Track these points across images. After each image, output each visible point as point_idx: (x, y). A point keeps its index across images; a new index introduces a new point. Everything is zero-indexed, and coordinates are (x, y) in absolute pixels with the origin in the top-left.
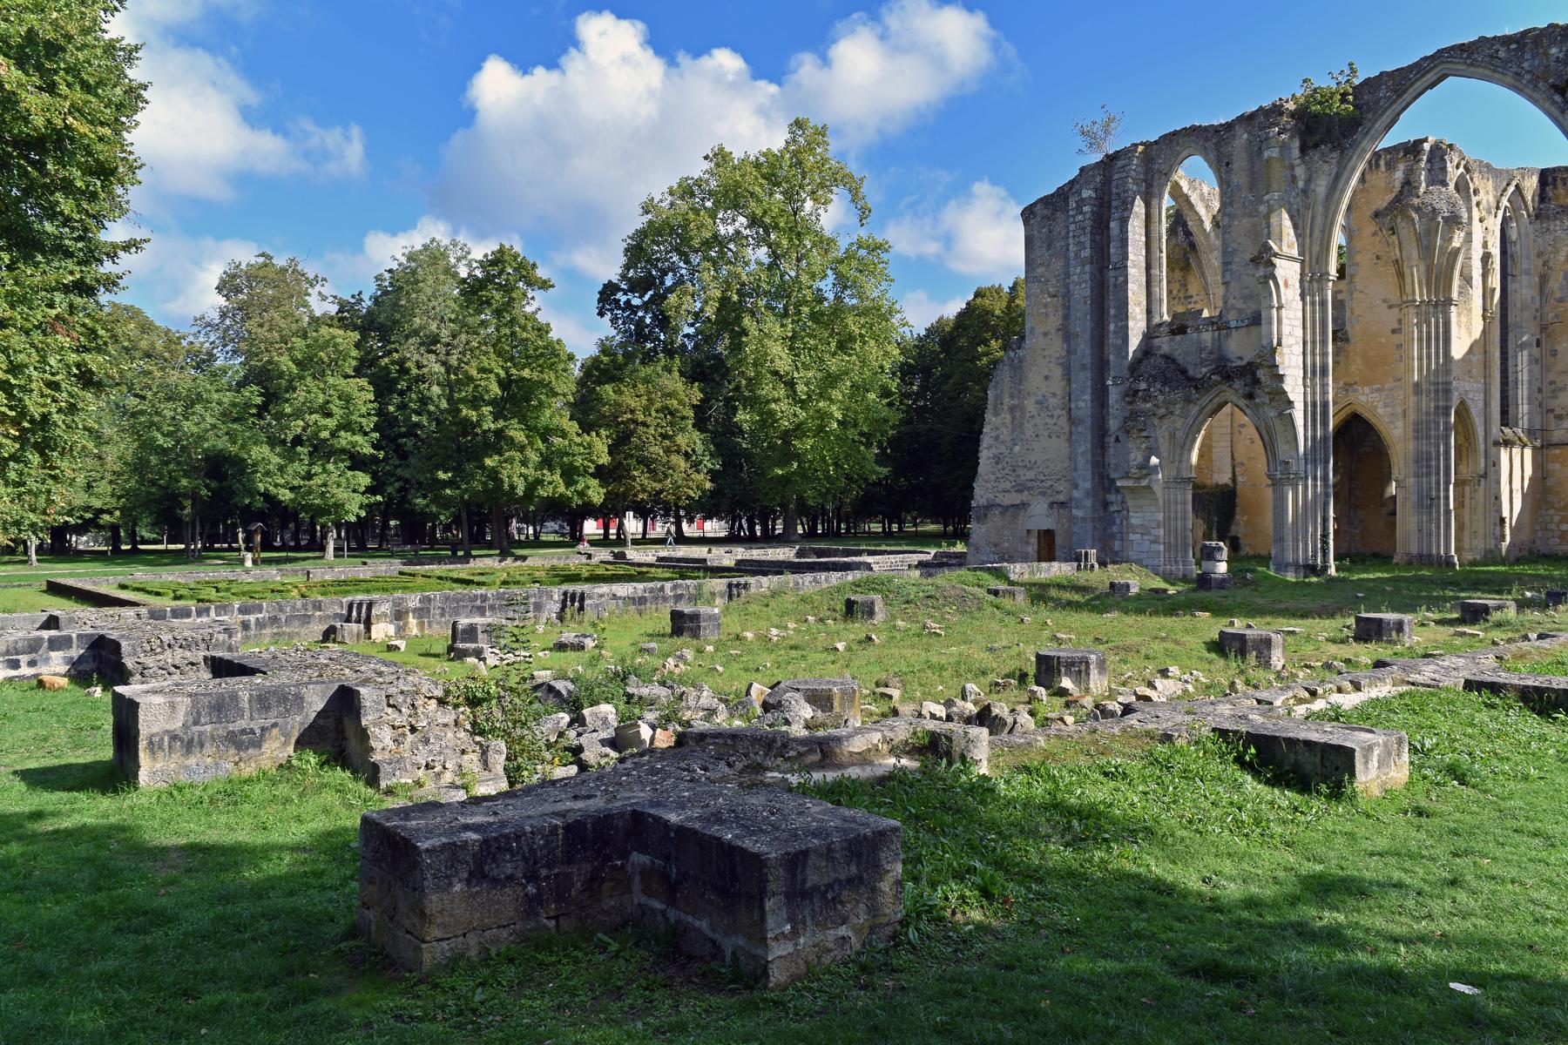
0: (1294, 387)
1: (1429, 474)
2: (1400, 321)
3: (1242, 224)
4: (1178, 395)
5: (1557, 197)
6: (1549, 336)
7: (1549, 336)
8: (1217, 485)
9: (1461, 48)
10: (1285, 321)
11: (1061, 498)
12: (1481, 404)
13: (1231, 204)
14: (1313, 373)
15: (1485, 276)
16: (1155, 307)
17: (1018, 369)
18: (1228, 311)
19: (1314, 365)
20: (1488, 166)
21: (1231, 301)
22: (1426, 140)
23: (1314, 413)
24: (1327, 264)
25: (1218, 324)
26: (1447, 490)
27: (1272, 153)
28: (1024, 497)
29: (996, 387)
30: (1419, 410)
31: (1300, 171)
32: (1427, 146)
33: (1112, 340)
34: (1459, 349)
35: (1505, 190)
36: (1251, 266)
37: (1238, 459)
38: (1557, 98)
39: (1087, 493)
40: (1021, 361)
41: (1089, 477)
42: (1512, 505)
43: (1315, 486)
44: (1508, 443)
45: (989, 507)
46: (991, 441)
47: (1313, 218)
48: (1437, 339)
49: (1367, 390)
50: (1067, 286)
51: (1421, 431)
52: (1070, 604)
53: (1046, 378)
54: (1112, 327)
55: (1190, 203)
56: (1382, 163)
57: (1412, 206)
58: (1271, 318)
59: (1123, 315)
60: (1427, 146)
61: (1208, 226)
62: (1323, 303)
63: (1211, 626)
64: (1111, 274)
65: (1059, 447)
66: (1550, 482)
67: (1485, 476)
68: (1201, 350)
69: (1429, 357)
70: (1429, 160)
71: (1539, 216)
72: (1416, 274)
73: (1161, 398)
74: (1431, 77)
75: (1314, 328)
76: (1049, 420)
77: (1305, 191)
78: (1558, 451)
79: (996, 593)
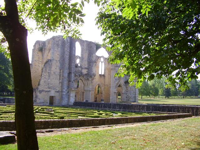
46: (44, 78)
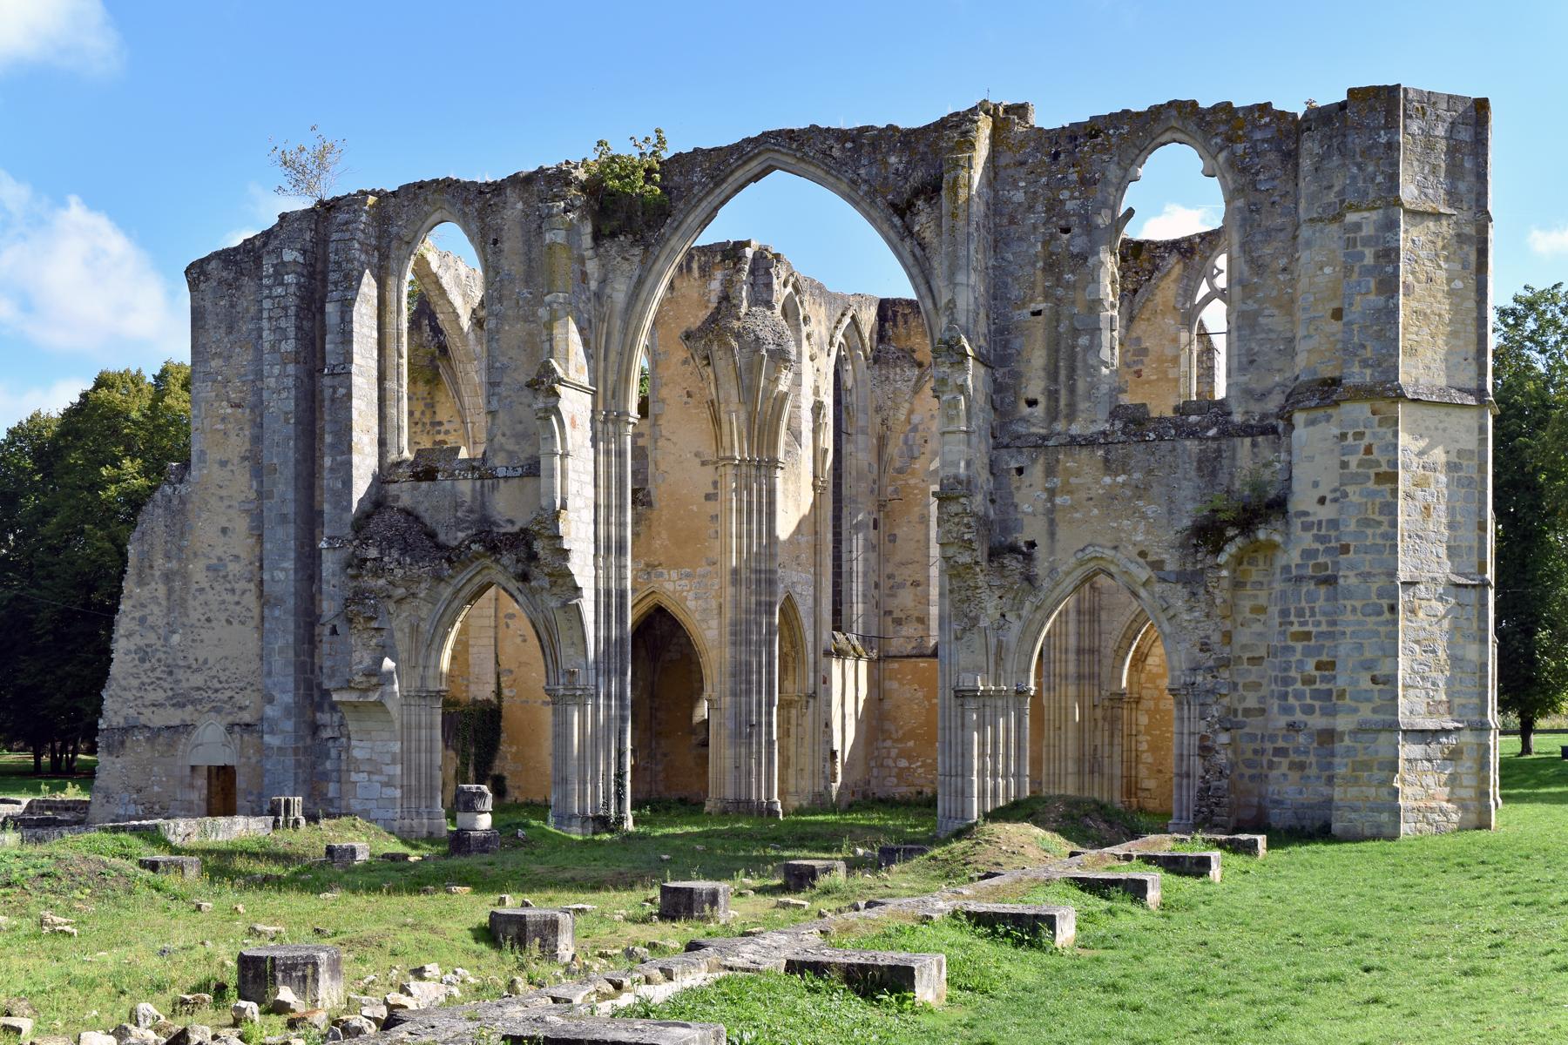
0: (582, 568)
1: (749, 692)
2: (715, 484)
3: (514, 331)
4: (423, 569)
5: (898, 338)
6: (887, 515)
7: (887, 515)
8: (475, 702)
9: (790, 135)
10: (571, 475)
11: (246, 717)
12: (810, 601)
13: (500, 302)
14: (608, 549)
15: (816, 431)
16: (391, 438)
17: (178, 514)
18: (495, 452)
19: (608, 537)
20: (820, 287)
21: (499, 439)
22: (748, 244)
23: (608, 606)
24: (626, 400)
25: (480, 469)
26: (770, 714)
27: (556, 236)
28: (186, 714)
29: (141, 539)
30: (737, 604)
31: (592, 267)
32: (749, 252)
33: (328, 481)
34: (785, 526)
35: (839, 321)
36: (527, 391)
37: (505, 665)
38: (896, 220)
39: (287, 711)
40: (183, 501)
41: (291, 686)
42: (844, 735)
43: (608, 707)
44: (840, 654)
45: (128, 730)
46: (134, 626)
47: (609, 335)
48: (760, 512)
49: (674, 574)
50: (258, 393)
51: (740, 634)
52: (276, 883)
53: (224, 531)
54: (327, 462)
55: (440, 287)
56: (695, 266)
57: (732, 330)
58: (553, 469)
59: (344, 445)
60: (749, 252)
61: (465, 323)
62: (621, 454)
63: (475, 907)
64: (327, 381)
65: (243, 640)
66: (887, 705)
67: (814, 695)
68: (457, 506)
69: (750, 536)
70: (752, 272)
71: (877, 359)
72: (735, 421)
73: (399, 572)
74: (754, 166)
75: (608, 487)
76: (229, 597)
77: (598, 296)
78: (896, 666)
79: (154, 866)
